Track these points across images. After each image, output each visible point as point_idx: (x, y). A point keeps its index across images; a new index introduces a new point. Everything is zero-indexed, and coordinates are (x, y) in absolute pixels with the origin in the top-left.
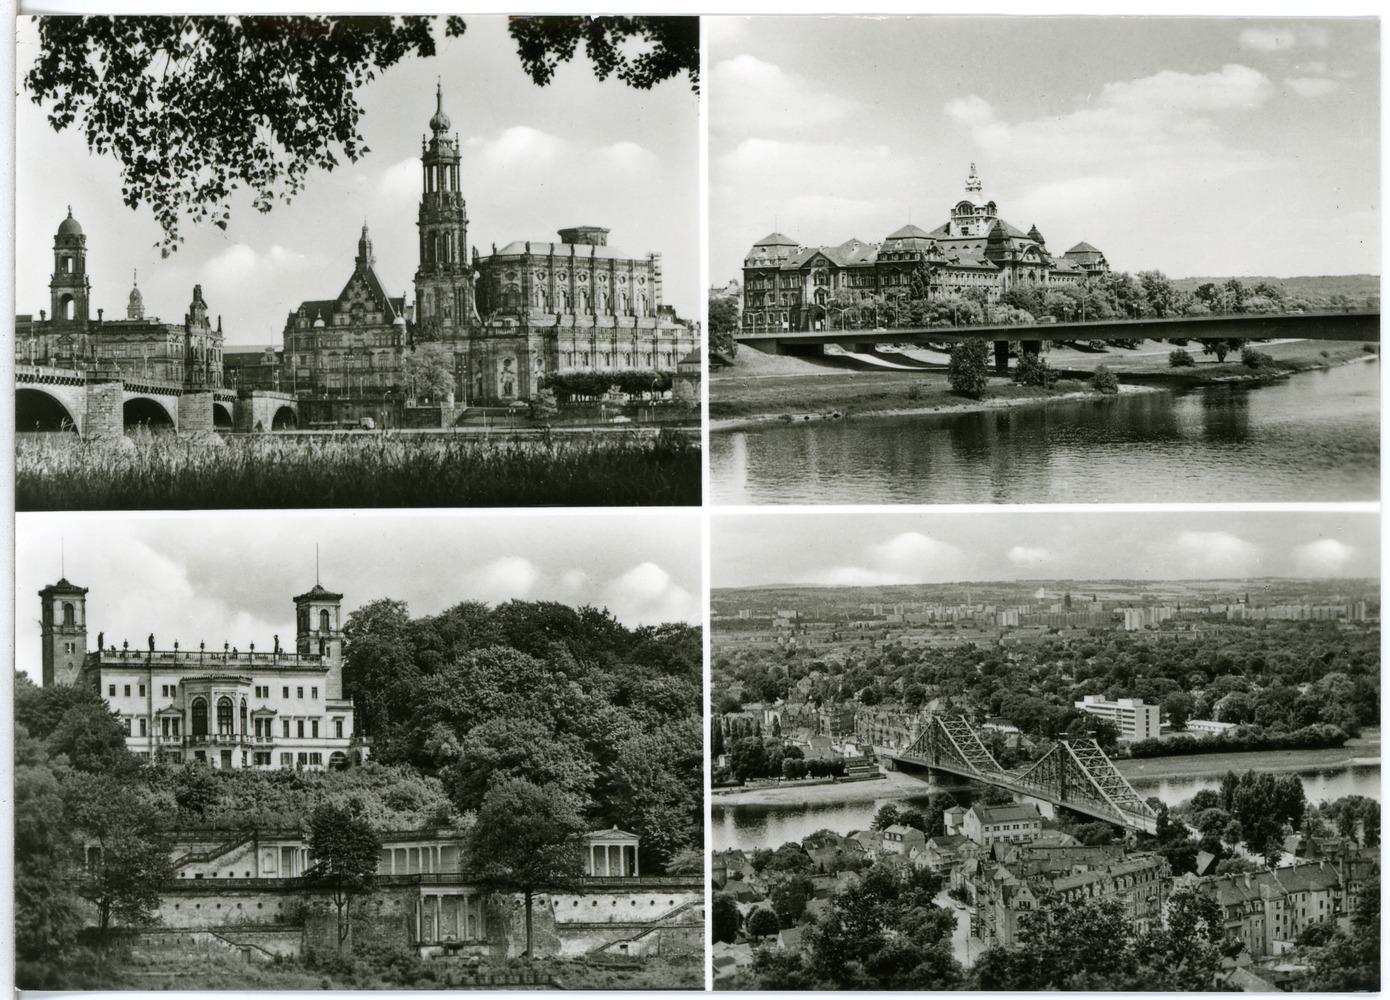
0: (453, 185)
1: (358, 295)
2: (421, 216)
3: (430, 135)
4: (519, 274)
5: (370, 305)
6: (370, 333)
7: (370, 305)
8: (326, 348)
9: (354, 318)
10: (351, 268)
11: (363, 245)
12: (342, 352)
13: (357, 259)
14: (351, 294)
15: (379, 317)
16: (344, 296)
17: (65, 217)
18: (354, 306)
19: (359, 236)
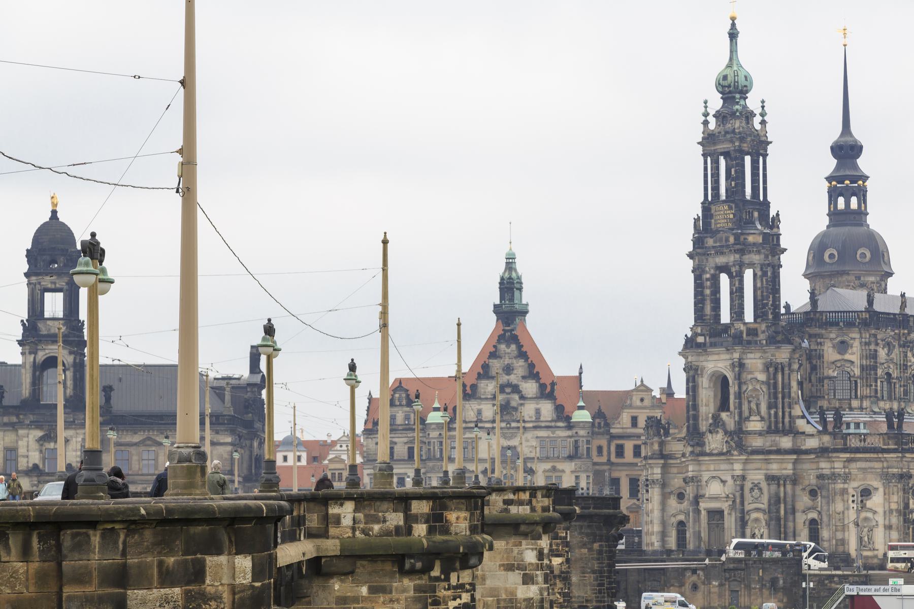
0: (755, 189)
1: (508, 370)
2: (698, 242)
3: (716, 103)
4: (856, 344)
5: (530, 388)
6: (529, 435)
7: (530, 388)
9: (506, 409)
10: (489, 323)
11: (510, 286)
13: (497, 309)
14: (496, 366)
15: (547, 409)
16: (484, 371)
19: (500, 269)
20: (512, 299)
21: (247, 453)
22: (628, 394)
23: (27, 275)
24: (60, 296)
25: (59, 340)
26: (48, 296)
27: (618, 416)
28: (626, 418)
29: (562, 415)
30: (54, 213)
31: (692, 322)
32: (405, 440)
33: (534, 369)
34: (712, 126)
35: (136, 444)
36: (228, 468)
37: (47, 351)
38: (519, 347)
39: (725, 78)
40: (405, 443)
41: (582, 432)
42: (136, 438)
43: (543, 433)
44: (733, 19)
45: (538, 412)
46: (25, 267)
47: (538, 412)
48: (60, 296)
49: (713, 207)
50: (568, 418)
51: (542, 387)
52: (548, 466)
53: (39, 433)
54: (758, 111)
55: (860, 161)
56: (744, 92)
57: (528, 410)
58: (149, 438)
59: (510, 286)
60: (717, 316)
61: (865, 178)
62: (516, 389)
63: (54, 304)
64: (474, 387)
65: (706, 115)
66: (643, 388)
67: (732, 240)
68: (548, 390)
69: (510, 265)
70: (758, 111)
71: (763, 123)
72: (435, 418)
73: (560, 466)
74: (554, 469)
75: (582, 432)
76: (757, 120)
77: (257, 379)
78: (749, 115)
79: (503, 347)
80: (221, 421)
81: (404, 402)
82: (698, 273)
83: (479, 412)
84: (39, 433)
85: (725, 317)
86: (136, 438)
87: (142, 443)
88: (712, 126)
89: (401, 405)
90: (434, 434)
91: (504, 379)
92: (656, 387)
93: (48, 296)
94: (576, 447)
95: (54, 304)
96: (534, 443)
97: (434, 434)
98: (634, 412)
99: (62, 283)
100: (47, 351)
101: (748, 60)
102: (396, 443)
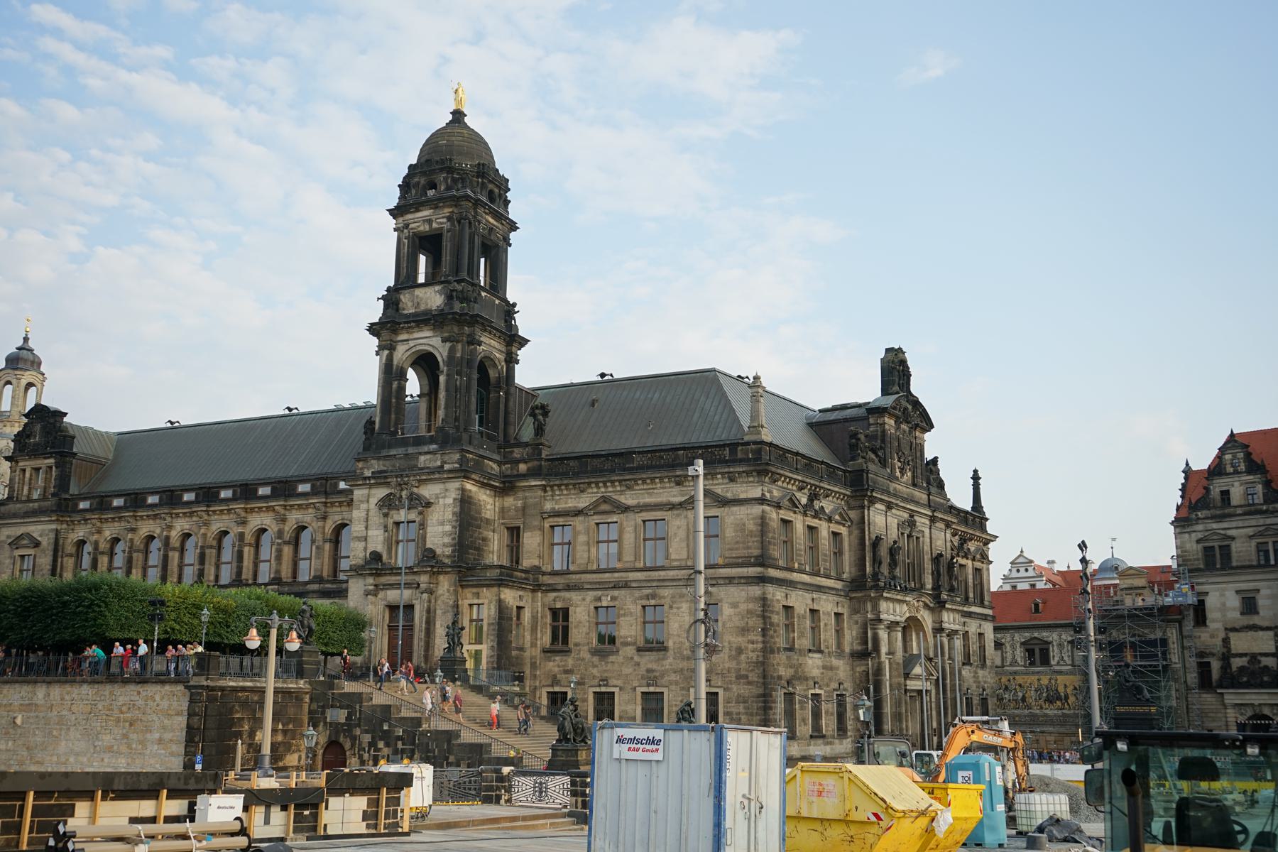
21: (856, 532)
32: (1250, 531)
35: (578, 513)
36: (756, 552)
37: (412, 343)
40: (1251, 537)
42: (583, 501)
53: (381, 492)
58: (605, 500)
80: (740, 455)
81: (1242, 467)
84: (381, 492)
86: (583, 501)
87: (594, 509)
89: (1236, 472)
100: (412, 343)
102: (1233, 538)
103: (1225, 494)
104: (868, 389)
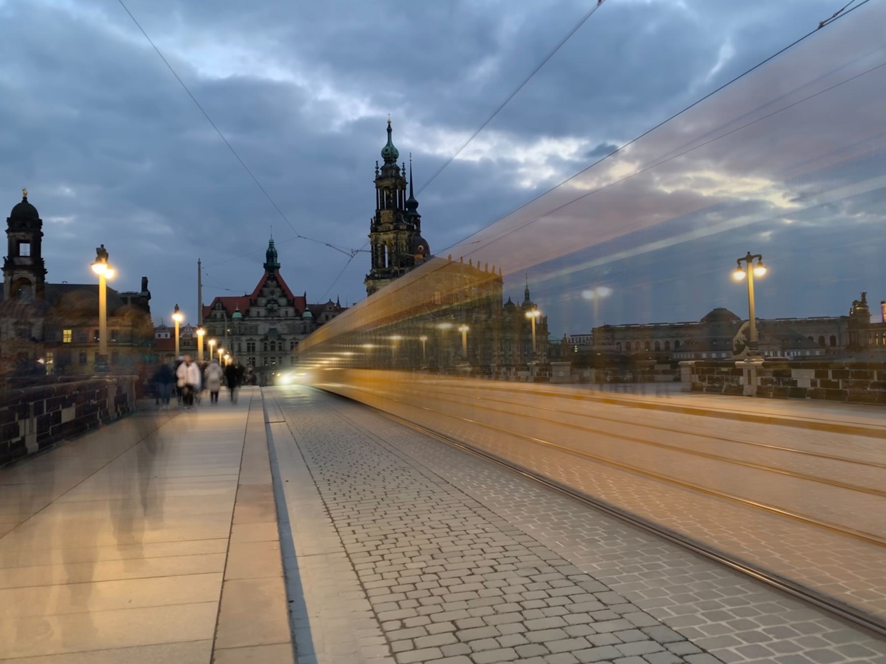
1: (272, 293)
3: (382, 163)
5: (283, 301)
6: (283, 323)
7: (283, 301)
8: (242, 335)
9: (271, 311)
10: (262, 272)
11: (271, 255)
12: (257, 338)
13: (265, 266)
14: (266, 291)
15: (291, 311)
16: (260, 291)
17: (20, 200)
18: (269, 302)
20: (273, 261)
22: (325, 305)
23: (7, 231)
24: (28, 245)
25: (27, 268)
26: (22, 245)
27: (320, 315)
28: (323, 315)
29: (298, 313)
30: (25, 199)
31: (370, 268)
33: (285, 292)
34: (380, 174)
38: (278, 282)
39: (386, 150)
41: (308, 322)
43: (289, 322)
44: (389, 123)
45: (287, 312)
46: (7, 227)
47: (287, 312)
48: (28, 245)
49: (382, 212)
50: (301, 315)
51: (289, 301)
52: (291, 337)
54: (401, 168)
55: (417, 210)
56: (396, 157)
57: (282, 312)
59: (271, 255)
60: (384, 266)
61: (420, 216)
62: (276, 302)
63: (25, 249)
64: (256, 301)
65: (377, 168)
66: (330, 303)
67: (392, 227)
68: (292, 301)
69: (271, 244)
70: (401, 168)
71: (404, 173)
72: (237, 315)
73: (297, 337)
74: (294, 339)
75: (308, 322)
76: (401, 172)
77: (146, 294)
78: (398, 169)
79: (269, 282)
82: (374, 244)
83: (258, 313)
84: (14, 320)
85: (387, 266)
88: (380, 174)
90: (236, 323)
91: (271, 297)
92: (335, 302)
93: (22, 245)
94: (305, 327)
95: (25, 249)
96: (285, 327)
97: (236, 323)
98: (327, 313)
99: (29, 237)
101: (396, 143)
103: (215, 315)
104: (138, 289)
